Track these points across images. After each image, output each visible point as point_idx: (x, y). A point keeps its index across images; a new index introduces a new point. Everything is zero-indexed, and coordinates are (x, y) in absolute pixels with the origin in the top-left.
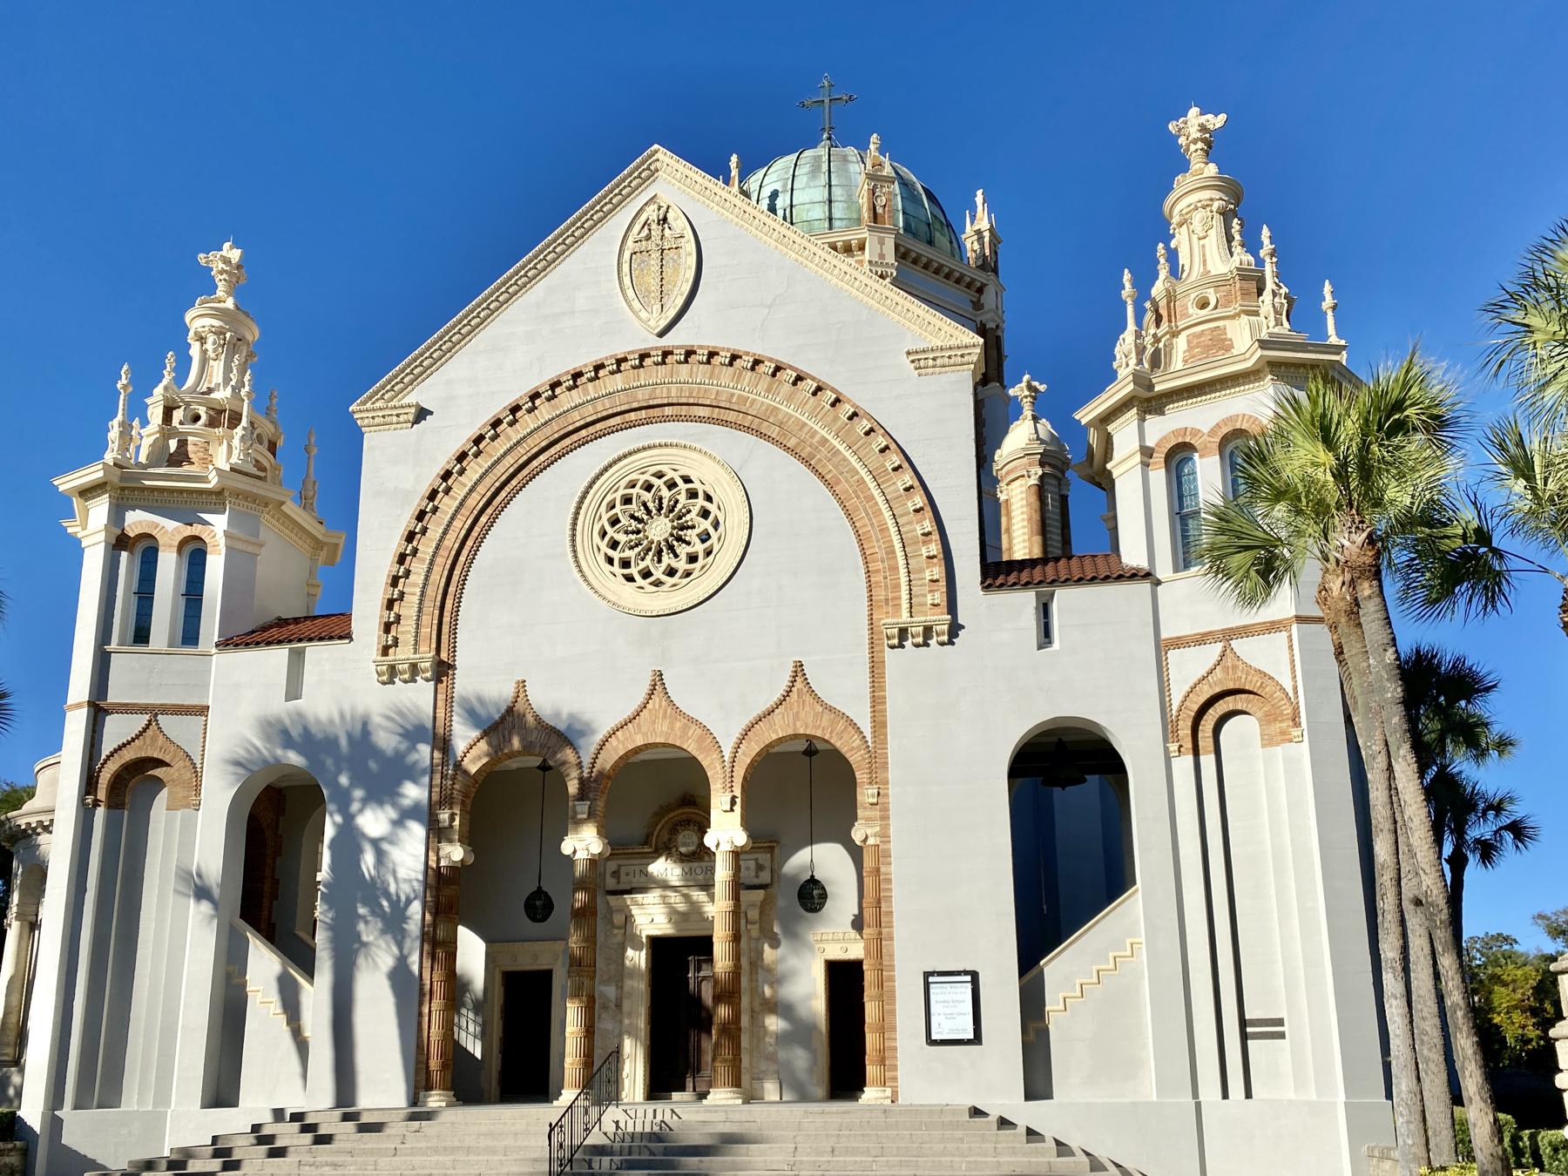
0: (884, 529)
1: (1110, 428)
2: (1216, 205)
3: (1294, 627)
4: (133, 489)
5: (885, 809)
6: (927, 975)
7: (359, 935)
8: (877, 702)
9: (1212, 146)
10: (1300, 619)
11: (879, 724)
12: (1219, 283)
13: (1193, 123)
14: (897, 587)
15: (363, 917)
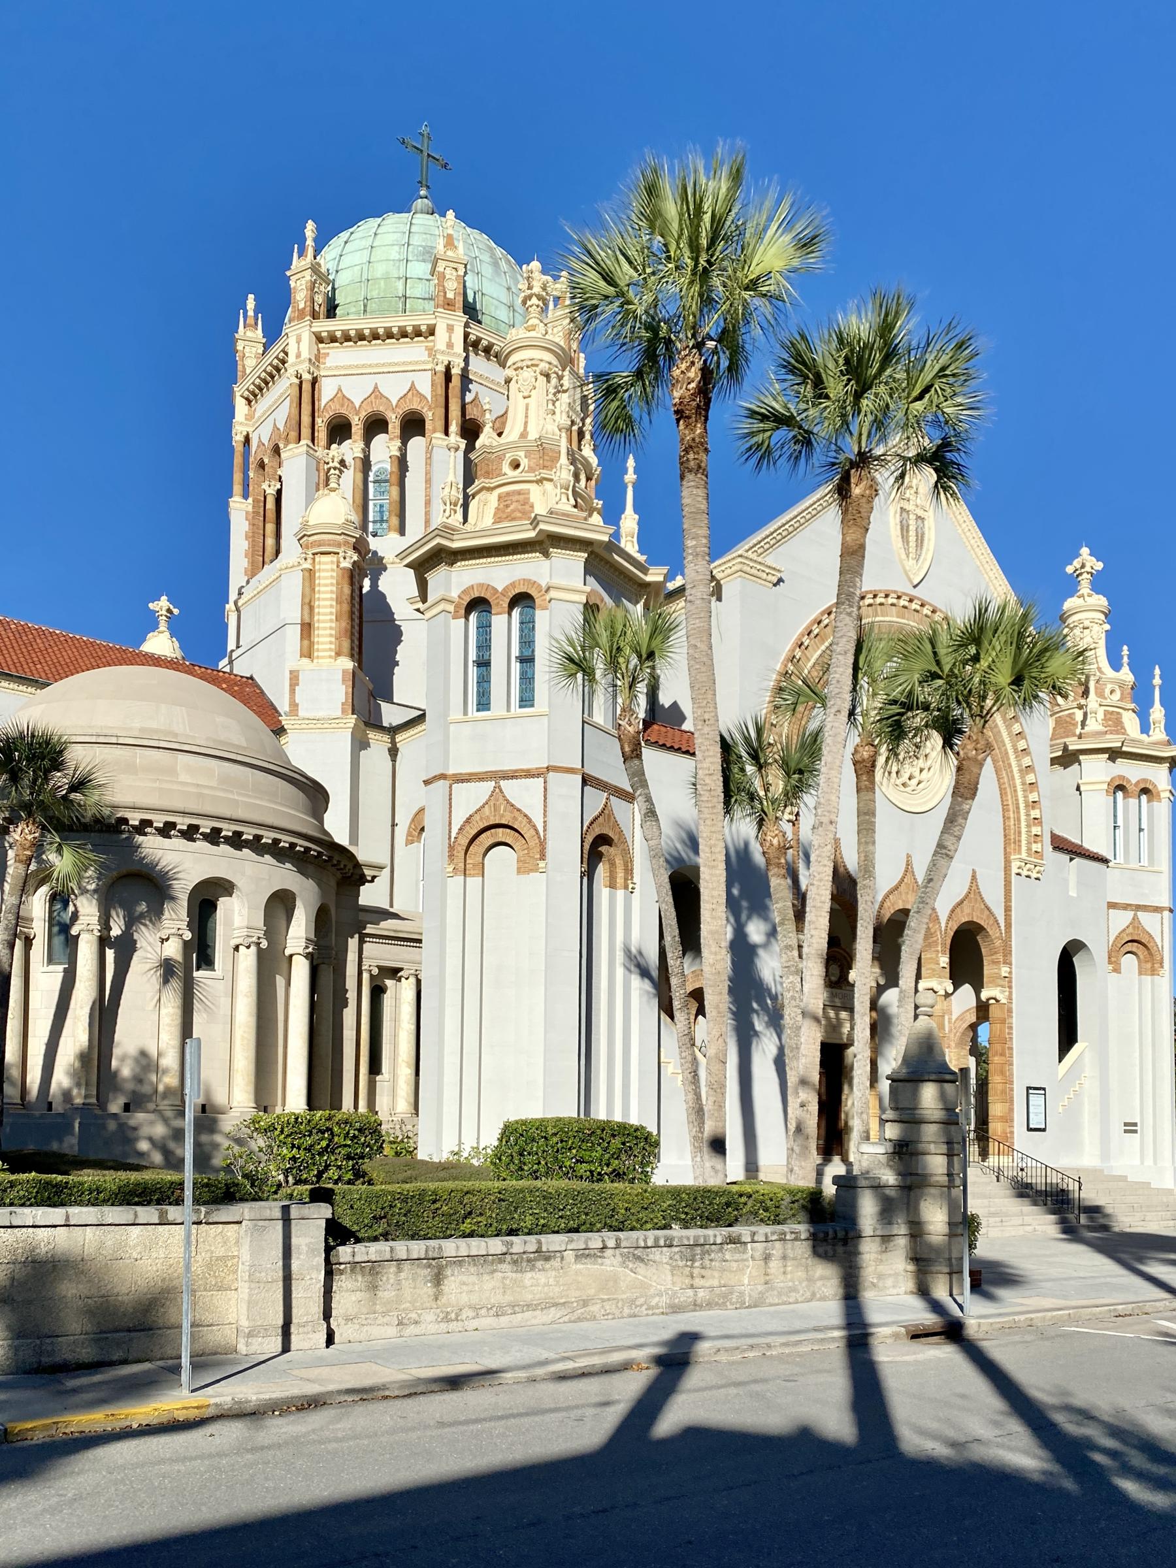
0: (1015, 791)
1: (1081, 757)
2: (1107, 627)
3: (1166, 913)
4: (602, 559)
5: (1010, 982)
6: (1028, 1088)
7: (753, 1025)
8: (1008, 909)
9: (1099, 583)
10: (1171, 911)
11: (1008, 925)
12: (1121, 686)
13: (1087, 561)
14: (1020, 833)
15: (756, 1012)
